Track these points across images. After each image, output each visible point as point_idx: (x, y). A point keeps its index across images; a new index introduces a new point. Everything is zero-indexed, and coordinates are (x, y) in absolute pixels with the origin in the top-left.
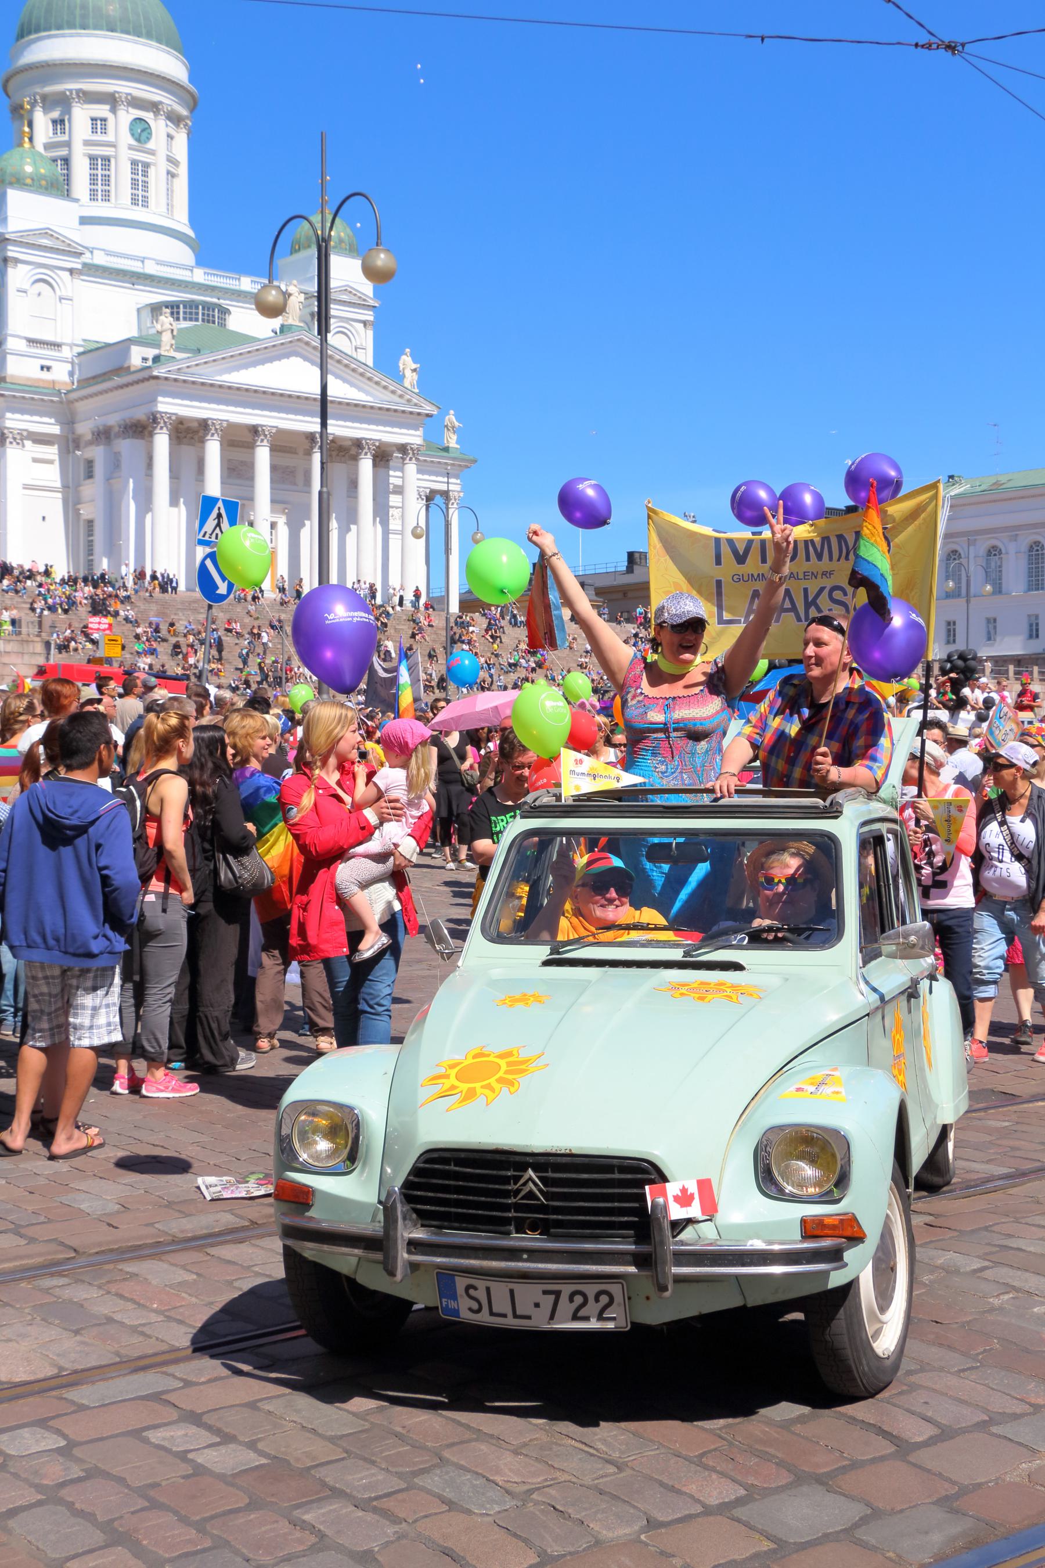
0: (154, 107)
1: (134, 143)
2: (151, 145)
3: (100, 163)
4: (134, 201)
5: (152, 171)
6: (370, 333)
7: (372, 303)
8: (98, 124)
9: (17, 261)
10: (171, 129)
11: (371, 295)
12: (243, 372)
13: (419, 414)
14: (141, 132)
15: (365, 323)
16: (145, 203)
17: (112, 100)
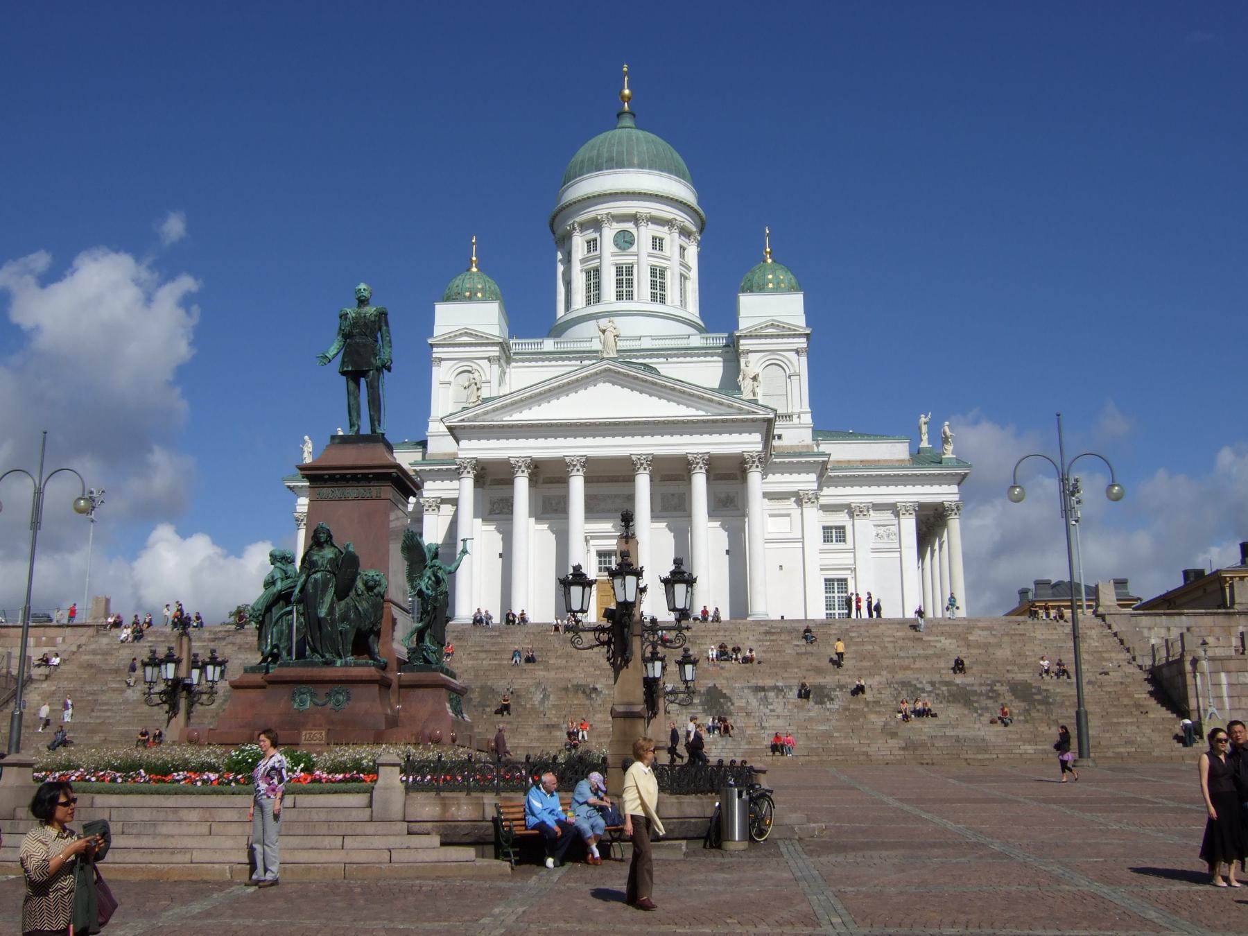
0: (635, 219)
1: (616, 250)
2: (634, 249)
3: (594, 276)
4: (619, 297)
5: (668, 274)
6: (804, 360)
7: (802, 331)
8: (592, 244)
9: (441, 360)
10: (661, 231)
11: (804, 325)
12: (535, 409)
13: (753, 420)
14: (625, 241)
15: (797, 352)
16: (630, 296)
17: (596, 224)
